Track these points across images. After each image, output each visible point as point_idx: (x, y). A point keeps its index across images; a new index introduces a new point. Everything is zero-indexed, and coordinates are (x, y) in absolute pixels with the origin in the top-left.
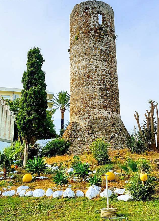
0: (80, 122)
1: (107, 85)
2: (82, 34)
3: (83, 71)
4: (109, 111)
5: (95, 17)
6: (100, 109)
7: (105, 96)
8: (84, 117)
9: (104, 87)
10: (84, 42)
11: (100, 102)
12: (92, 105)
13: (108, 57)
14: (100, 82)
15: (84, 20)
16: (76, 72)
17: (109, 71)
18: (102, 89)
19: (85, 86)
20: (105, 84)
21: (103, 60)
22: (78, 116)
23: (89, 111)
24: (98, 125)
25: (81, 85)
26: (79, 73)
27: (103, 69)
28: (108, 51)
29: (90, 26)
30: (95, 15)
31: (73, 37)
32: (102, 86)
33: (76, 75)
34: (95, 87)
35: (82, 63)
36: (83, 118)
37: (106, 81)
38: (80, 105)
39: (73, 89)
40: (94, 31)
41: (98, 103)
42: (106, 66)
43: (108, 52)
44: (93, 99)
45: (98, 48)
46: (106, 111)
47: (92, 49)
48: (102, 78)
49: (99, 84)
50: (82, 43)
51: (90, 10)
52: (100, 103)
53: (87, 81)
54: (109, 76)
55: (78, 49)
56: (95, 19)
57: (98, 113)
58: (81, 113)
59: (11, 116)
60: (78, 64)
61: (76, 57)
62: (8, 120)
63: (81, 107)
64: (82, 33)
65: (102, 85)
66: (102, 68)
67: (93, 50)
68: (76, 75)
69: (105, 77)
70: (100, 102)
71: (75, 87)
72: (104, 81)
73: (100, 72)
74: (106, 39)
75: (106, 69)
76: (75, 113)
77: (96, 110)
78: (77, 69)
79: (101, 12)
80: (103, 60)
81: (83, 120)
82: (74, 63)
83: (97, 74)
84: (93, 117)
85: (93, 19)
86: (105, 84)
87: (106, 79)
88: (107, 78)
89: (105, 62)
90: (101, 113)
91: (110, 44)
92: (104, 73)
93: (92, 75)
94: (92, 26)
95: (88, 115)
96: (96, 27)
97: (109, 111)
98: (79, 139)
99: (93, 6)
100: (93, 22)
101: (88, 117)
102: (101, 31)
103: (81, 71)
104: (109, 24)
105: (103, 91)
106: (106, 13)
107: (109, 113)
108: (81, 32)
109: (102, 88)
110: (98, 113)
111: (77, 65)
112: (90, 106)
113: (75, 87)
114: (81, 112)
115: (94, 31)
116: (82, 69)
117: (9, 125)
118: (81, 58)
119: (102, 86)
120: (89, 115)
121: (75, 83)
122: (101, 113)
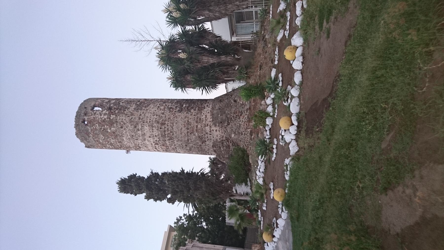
0: (214, 138)
1: (176, 105)
2: (112, 129)
3: (155, 130)
4: (206, 106)
6: (202, 114)
7: (189, 108)
8: (209, 132)
9: (178, 109)
10: (122, 127)
11: (194, 113)
12: (197, 122)
13: (144, 103)
14: (172, 112)
15: (96, 126)
16: (155, 140)
17: (161, 103)
18: (180, 111)
19: (173, 128)
20: (175, 108)
21: (147, 108)
22: (206, 140)
23: (202, 126)
24: (220, 115)
25: (172, 134)
26: (156, 136)
27: (158, 108)
28: (138, 103)
29: (105, 119)
30: (93, 113)
31: (114, 142)
32: (177, 110)
33: (158, 140)
34: (177, 118)
35: (146, 131)
37: (172, 107)
38: (194, 137)
39: (175, 145)
40: (111, 115)
41: (195, 115)
42: (154, 106)
43: (139, 103)
44: (189, 121)
45: (132, 112)
46: (205, 108)
47: (132, 118)
48: (168, 110)
49: (174, 113)
50: (122, 129)
51: (86, 118)
52: (195, 114)
53: (168, 126)
55: (129, 135)
57: (206, 116)
58: (204, 135)
59: (192, 246)
61: (137, 139)
63: (197, 136)
64: (110, 129)
65: (176, 110)
66: (156, 109)
67: (133, 117)
68: (158, 140)
69: (166, 107)
70: (194, 113)
71: (172, 142)
72: (171, 108)
73: (161, 111)
74: (124, 104)
75: (158, 105)
76: (203, 143)
77: (202, 117)
78: (151, 138)
79: (91, 107)
81: (212, 134)
82: (144, 142)
83: (162, 115)
84: (210, 121)
85: (97, 116)
86: (175, 108)
87: (169, 107)
89: (150, 106)
90: (207, 113)
92: (162, 108)
93: (162, 120)
94: (106, 117)
95: (207, 127)
96: (107, 112)
97: (206, 106)
99: (82, 115)
100: (101, 115)
101: (209, 127)
103: (156, 133)
105: (182, 110)
108: (109, 131)
110: (206, 116)
111: (147, 137)
112: (197, 124)
113: (172, 142)
114: (202, 136)
115: (111, 115)
116: (153, 132)
117: (203, 249)
118: (140, 132)
119: (177, 110)
121: (167, 142)
122: (207, 113)
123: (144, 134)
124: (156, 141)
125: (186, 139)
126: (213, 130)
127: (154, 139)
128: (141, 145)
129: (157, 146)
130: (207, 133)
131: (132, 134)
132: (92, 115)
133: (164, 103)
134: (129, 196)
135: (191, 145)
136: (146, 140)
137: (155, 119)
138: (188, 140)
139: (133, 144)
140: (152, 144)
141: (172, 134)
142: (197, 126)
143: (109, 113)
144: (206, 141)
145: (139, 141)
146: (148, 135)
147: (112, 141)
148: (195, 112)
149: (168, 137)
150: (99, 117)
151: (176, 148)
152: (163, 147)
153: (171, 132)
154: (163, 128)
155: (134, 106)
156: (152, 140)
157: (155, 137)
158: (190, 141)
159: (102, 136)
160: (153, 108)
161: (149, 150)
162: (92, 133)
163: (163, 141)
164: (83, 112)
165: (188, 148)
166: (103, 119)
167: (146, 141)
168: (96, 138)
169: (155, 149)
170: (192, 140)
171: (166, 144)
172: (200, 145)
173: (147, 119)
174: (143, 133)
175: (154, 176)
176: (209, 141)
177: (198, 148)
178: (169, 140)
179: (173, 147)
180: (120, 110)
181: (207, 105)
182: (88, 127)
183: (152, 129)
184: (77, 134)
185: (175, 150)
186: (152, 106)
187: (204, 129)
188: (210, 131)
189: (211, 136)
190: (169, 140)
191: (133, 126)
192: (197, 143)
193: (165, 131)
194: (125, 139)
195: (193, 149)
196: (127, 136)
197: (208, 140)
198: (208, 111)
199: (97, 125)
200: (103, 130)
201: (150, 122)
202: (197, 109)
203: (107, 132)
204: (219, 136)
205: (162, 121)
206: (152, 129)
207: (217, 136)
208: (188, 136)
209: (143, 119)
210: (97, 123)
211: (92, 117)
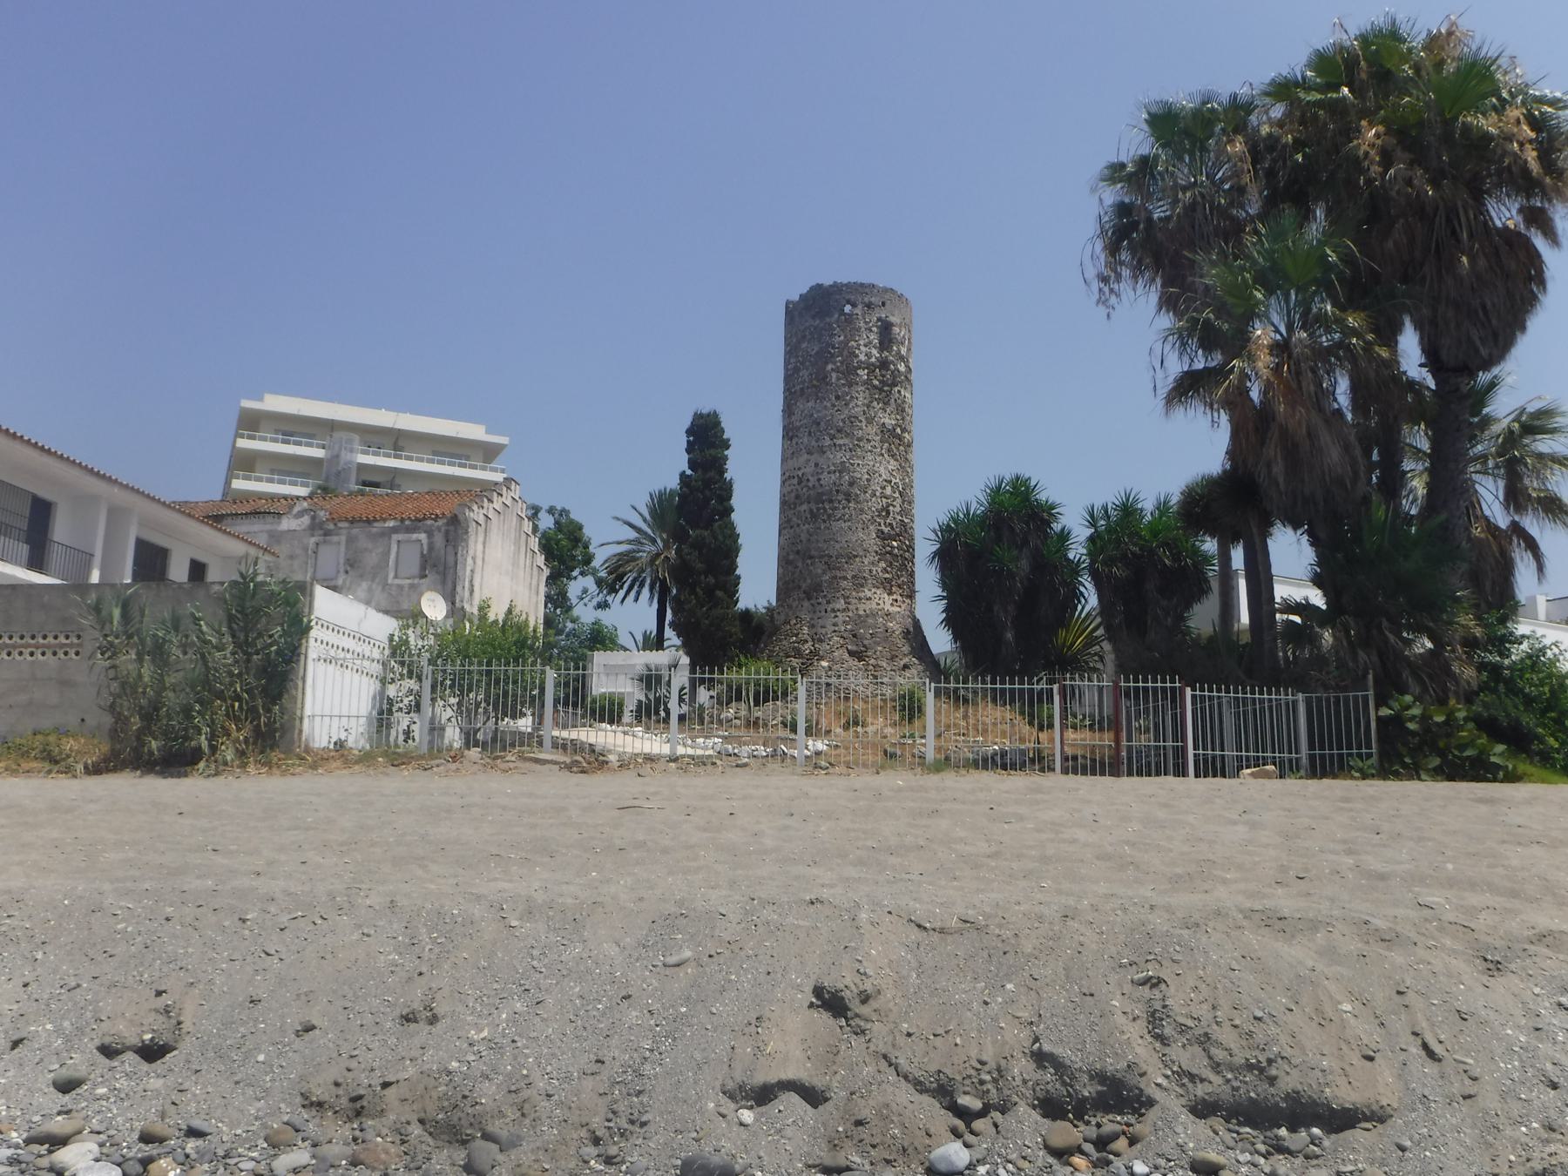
2: (834, 375)
4: (895, 597)
5: (871, 331)
6: (873, 590)
9: (886, 530)
10: (838, 398)
12: (854, 577)
16: (810, 478)
18: (881, 536)
21: (886, 456)
25: (825, 517)
26: (819, 480)
28: (898, 431)
29: (857, 356)
32: (883, 527)
33: (810, 485)
35: (832, 456)
36: (829, 609)
38: (820, 571)
39: (798, 525)
40: (866, 371)
41: (870, 571)
44: (857, 559)
46: (889, 594)
47: (861, 421)
51: (858, 311)
53: (844, 508)
54: (899, 500)
56: (872, 338)
57: (870, 599)
60: (815, 455)
62: (534, 582)
67: (864, 424)
68: (810, 485)
72: (888, 513)
75: (894, 481)
76: (805, 592)
80: (886, 456)
84: (857, 609)
87: (891, 508)
88: (894, 506)
91: (903, 410)
92: (888, 491)
94: (862, 357)
95: (842, 601)
96: (873, 360)
97: (895, 597)
98: (825, 664)
99: (866, 300)
100: (865, 346)
102: (884, 372)
104: (903, 351)
105: (884, 539)
106: (898, 321)
107: (896, 601)
108: (830, 367)
109: (883, 532)
110: (870, 599)
111: (815, 458)
116: (829, 473)
118: (828, 442)
120: (846, 603)
121: (805, 507)
123: (824, 453)
124: (808, 480)
125: (813, 553)
126: (836, 616)
127: (812, 476)
128: (797, 443)
129: (795, 481)
130: (828, 602)
131: (822, 423)
132: (866, 323)
133: (900, 492)
134: (682, 441)
135: (800, 564)
136: (809, 457)
137: (859, 476)
138: (811, 557)
139: (798, 424)
140: (799, 469)
141: (825, 517)
142: (845, 578)
143: (873, 364)
144: (809, 600)
145: (806, 440)
146: (821, 461)
147: (804, 373)
148: (879, 570)
149: (818, 509)
150: (862, 342)
151: (791, 527)
152: (793, 495)
153: (829, 516)
154: (839, 498)
155: (889, 421)
156: (809, 469)
157: (816, 478)
158: (809, 562)
159: (816, 349)
160: (886, 468)
161: (784, 460)
162: (822, 325)
163: (808, 497)
164: (873, 299)
165: (791, 557)
166: (857, 352)
167: (806, 456)
168: (811, 333)
169: (787, 474)
170: (812, 568)
171: (801, 504)
172: (800, 587)
173: (858, 457)
174: (825, 449)
175: (726, 491)
176: (811, 607)
177: (793, 582)
178: (811, 511)
179: (795, 519)
180: (881, 390)
181: (896, 601)
182: (836, 316)
183: (835, 472)
184: (819, 286)
185: (785, 525)
186: (893, 464)
187: (838, 595)
188: (833, 610)
189: (823, 613)
190: (811, 511)
191: (841, 424)
192: (805, 580)
193: (831, 501)
194: (810, 404)
195: (790, 568)
196: (819, 411)
197: (813, 605)
198: (881, 602)
199: (842, 338)
200: (830, 353)
201: (852, 465)
202: (887, 576)
203: (827, 363)
204: (823, 631)
205: (857, 495)
206: (835, 472)
207: (822, 627)
208: (821, 557)
209: (860, 447)
210: (845, 337)
211: (862, 324)
